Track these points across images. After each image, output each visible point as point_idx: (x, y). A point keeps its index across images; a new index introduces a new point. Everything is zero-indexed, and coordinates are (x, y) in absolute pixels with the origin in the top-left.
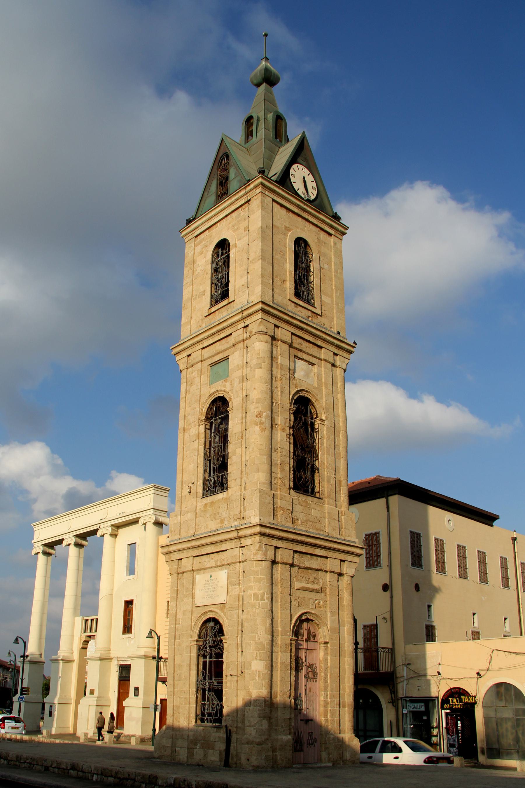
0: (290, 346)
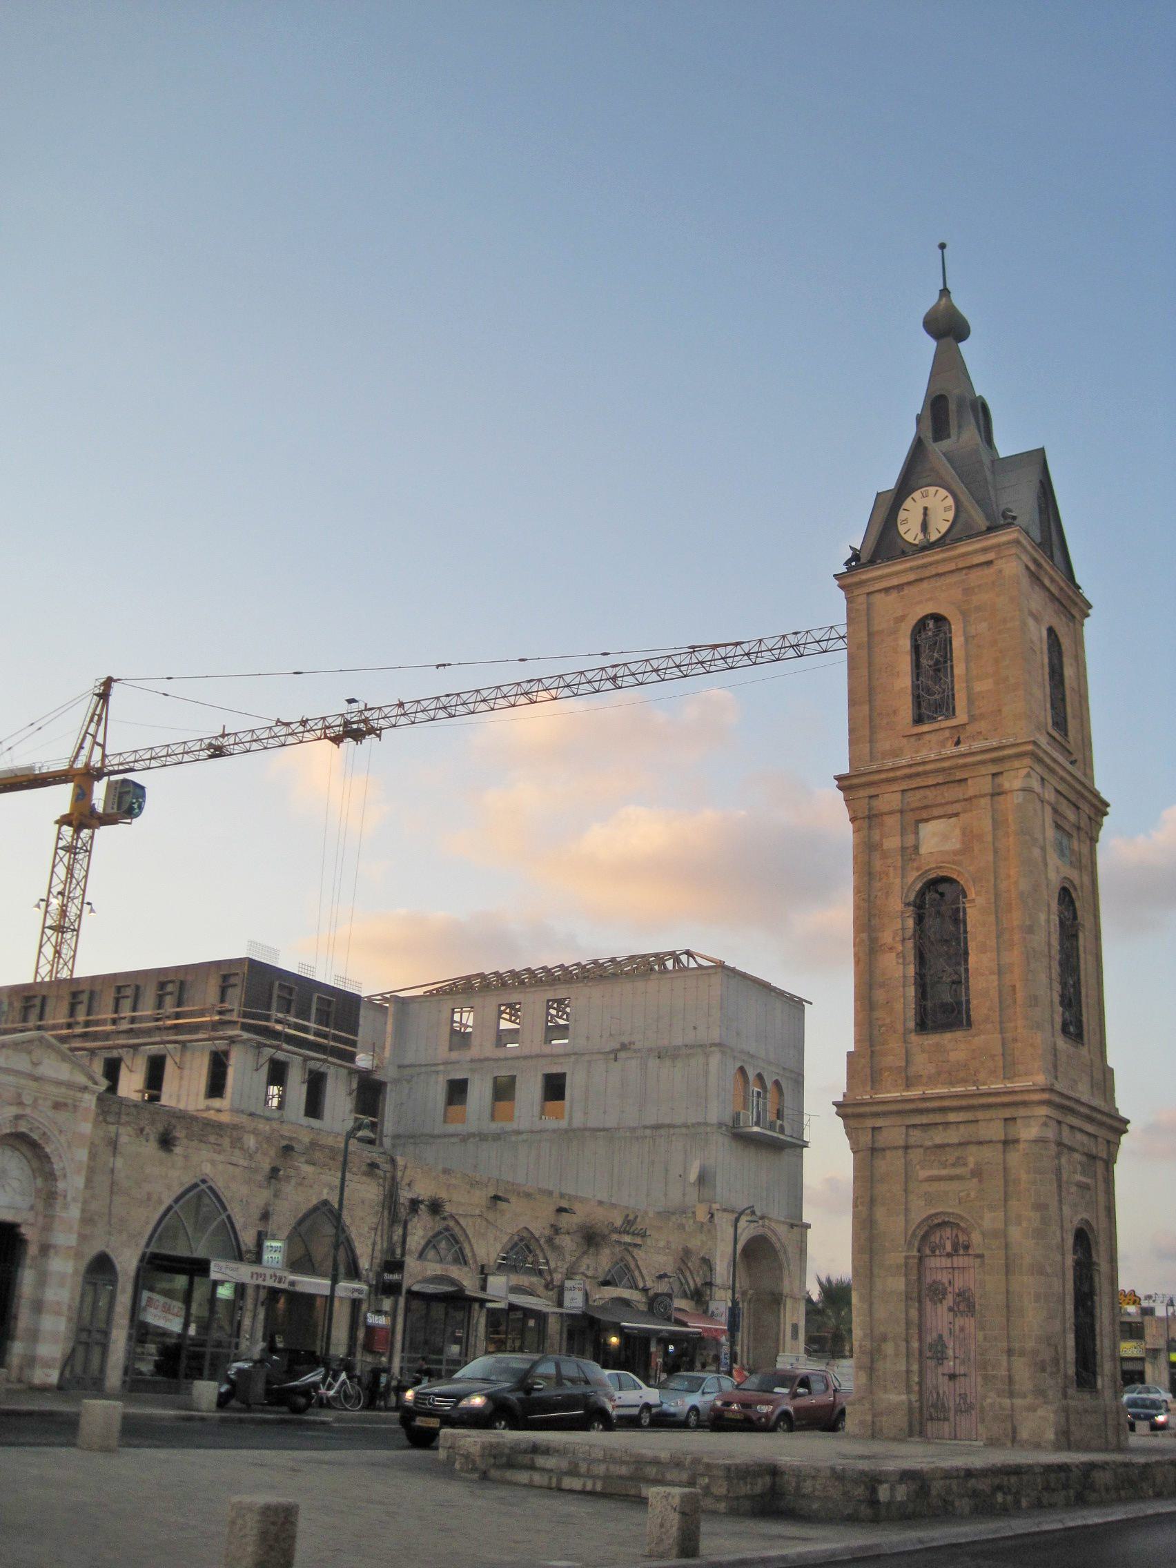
0: (902, 812)
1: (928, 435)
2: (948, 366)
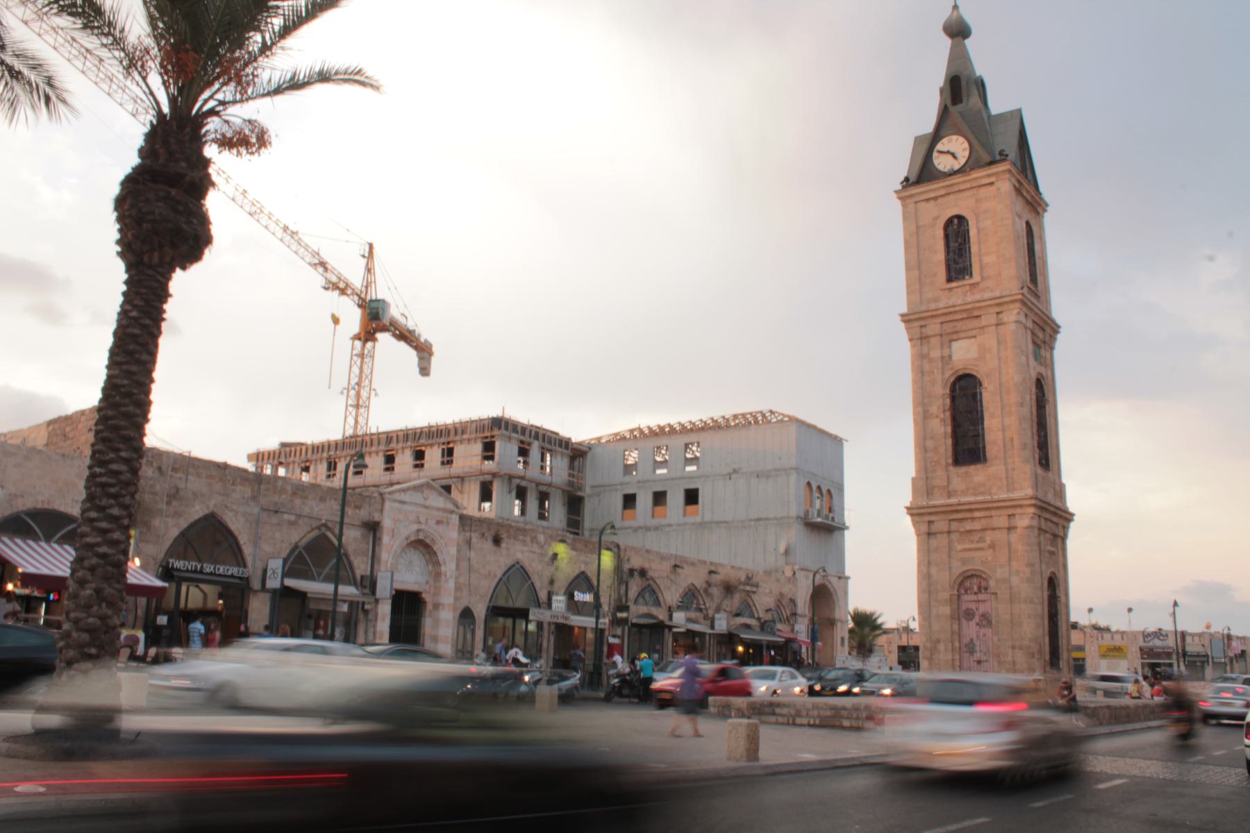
1: (949, 102)
2: (959, 58)
